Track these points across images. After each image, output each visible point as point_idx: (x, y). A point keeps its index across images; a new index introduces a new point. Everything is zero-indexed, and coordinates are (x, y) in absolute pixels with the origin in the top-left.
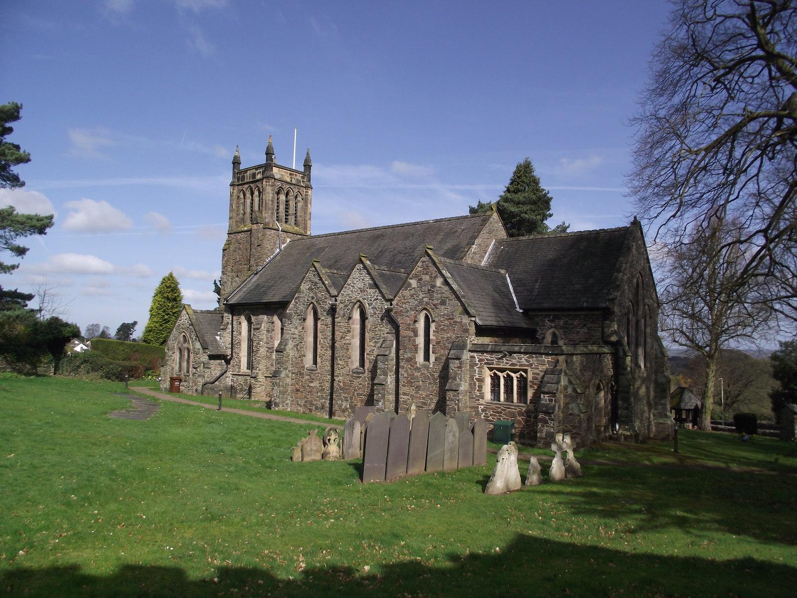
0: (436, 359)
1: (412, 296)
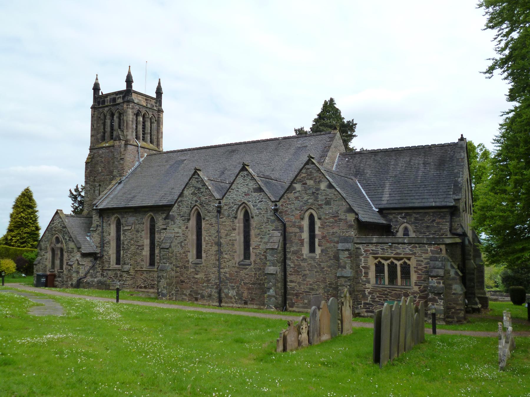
0: (322, 251)
1: (297, 198)
